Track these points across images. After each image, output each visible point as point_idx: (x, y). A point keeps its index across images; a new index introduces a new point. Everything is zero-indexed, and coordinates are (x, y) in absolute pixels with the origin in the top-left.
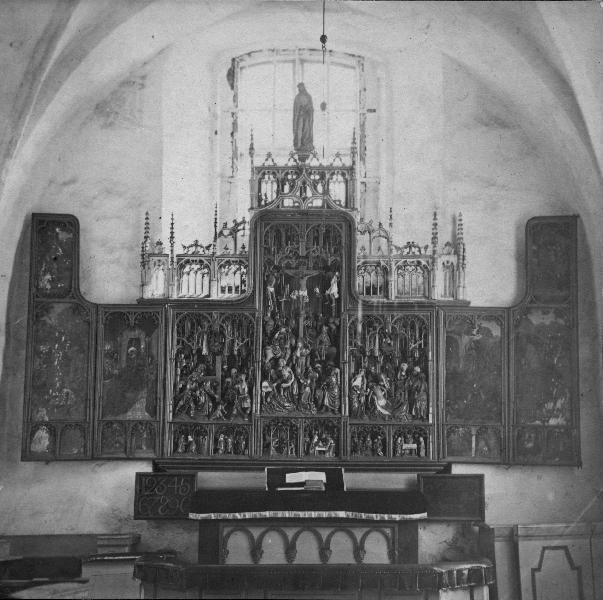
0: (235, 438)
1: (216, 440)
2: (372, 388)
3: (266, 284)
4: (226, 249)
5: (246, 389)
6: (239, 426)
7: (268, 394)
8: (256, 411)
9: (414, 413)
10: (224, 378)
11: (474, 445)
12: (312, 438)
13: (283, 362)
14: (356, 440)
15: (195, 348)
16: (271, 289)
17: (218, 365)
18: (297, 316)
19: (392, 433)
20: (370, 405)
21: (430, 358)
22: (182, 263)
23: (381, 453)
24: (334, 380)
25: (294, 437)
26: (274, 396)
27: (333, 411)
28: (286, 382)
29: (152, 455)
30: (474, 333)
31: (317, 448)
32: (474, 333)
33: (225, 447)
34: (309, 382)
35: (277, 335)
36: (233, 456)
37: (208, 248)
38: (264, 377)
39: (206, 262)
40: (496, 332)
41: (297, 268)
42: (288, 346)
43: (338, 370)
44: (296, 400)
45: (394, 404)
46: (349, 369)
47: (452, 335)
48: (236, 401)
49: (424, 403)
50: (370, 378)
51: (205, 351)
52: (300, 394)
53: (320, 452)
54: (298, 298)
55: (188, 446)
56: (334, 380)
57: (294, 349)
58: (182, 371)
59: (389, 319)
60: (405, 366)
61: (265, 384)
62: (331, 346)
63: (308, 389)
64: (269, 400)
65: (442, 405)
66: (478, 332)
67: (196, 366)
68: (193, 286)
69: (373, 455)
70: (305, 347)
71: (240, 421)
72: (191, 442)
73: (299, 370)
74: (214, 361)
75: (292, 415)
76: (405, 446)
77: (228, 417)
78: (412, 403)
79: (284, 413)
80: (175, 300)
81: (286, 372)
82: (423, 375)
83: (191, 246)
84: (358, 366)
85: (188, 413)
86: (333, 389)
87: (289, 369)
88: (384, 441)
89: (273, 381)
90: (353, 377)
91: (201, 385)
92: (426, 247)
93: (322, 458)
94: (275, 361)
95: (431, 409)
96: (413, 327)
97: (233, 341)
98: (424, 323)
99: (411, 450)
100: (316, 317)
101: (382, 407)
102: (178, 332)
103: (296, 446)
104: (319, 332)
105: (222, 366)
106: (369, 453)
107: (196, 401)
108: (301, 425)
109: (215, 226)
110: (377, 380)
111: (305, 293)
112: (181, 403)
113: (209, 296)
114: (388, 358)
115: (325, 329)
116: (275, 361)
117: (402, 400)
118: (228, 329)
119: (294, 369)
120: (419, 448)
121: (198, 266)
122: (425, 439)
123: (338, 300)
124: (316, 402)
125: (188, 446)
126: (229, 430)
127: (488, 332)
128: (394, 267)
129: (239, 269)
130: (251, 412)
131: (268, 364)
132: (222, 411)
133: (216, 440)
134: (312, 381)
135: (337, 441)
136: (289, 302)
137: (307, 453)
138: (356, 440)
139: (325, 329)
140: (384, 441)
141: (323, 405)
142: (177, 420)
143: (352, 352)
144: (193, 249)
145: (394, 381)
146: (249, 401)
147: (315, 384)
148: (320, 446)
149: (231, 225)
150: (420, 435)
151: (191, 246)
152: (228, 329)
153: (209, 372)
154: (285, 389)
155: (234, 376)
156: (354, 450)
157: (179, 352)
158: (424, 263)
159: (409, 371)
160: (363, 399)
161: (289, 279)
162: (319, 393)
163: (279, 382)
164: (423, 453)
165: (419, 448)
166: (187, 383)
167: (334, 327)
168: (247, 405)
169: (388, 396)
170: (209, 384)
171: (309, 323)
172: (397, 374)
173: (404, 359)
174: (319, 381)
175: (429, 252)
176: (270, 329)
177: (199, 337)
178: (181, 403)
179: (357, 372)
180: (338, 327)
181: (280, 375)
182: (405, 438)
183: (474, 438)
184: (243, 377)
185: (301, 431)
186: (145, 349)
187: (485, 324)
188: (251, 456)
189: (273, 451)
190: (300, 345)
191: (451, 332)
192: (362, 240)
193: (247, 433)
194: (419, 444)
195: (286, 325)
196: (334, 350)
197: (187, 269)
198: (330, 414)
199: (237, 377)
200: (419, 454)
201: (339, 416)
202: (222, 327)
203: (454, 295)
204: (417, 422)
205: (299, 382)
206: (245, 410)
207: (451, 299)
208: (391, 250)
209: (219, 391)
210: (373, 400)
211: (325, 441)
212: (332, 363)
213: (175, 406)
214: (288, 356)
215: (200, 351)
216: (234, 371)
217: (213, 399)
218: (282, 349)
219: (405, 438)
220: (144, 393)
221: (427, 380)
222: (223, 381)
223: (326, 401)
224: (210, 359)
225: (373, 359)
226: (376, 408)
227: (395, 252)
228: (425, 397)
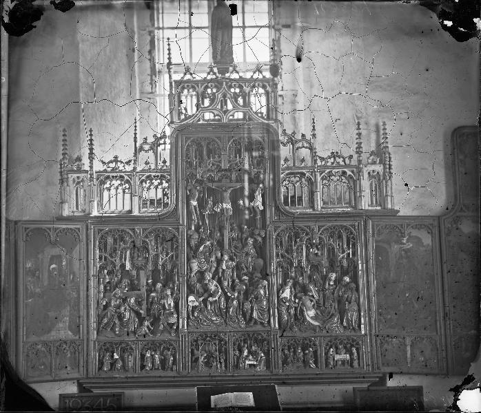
0: (162, 354)
1: (143, 356)
2: (300, 299)
3: (188, 199)
4: (147, 163)
5: (172, 304)
6: (165, 342)
7: (194, 308)
8: (183, 326)
9: (345, 324)
10: (149, 291)
11: (409, 353)
12: (241, 351)
13: (209, 276)
14: (286, 352)
15: (118, 263)
16: (194, 203)
17: (143, 281)
18: (221, 229)
19: (324, 345)
20: (299, 317)
21: (360, 268)
22: (103, 178)
23: (313, 366)
24: (262, 292)
28: (211, 295)
29: (76, 375)
30: (405, 241)
31: (247, 362)
32: (405, 241)
33: (153, 363)
34: (236, 294)
35: (201, 248)
36: (161, 373)
37: (128, 163)
38: (191, 291)
39: (126, 177)
40: (427, 240)
41: (220, 181)
42: (213, 259)
43: (266, 283)
44: (223, 313)
45: (324, 315)
46: (276, 280)
47: (380, 244)
48: (162, 317)
49: (355, 314)
50: (298, 289)
51: (128, 266)
52: (227, 308)
53: (250, 365)
54: (222, 210)
55: (113, 365)
56: (262, 292)
57: (219, 262)
58: (105, 287)
59: (316, 230)
60: (333, 276)
61: (191, 298)
62: (258, 258)
64: (196, 314)
65: (374, 315)
66: (408, 241)
67: (120, 281)
68: (115, 202)
69: (305, 367)
70: (231, 259)
71: (166, 337)
72: (117, 359)
73: (226, 284)
74: (138, 275)
76: (337, 357)
77: (152, 332)
78: (342, 313)
79: (213, 328)
80: (96, 217)
81: (212, 286)
82: (353, 285)
83: (111, 162)
84: (286, 277)
85: (113, 329)
86: (261, 301)
87: (215, 282)
88: (315, 352)
89: (198, 295)
90: (281, 288)
91: (125, 300)
92: (351, 157)
93: (252, 371)
94: (201, 274)
95: (362, 319)
96: (340, 237)
97: (157, 256)
98: (352, 233)
99: (343, 362)
100: (241, 229)
101: (312, 318)
102: (100, 249)
103: (226, 361)
104: (245, 245)
105: (147, 280)
106: (301, 364)
107: (121, 317)
108: (230, 339)
109: (135, 141)
110: (305, 290)
111: (229, 206)
112: (105, 320)
113: (130, 211)
114: (315, 267)
115: (251, 241)
116: (201, 274)
117: (333, 311)
118: (152, 244)
119: (220, 282)
120: (352, 359)
121: (119, 182)
122: (358, 350)
123: (263, 212)
124: (244, 315)
125: (113, 365)
126: (154, 346)
127: (419, 240)
128: (319, 178)
129: (161, 183)
130: (178, 327)
131: (194, 279)
132: (148, 327)
133: (143, 356)
134: (239, 293)
135: (267, 354)
136: (213, 216)
138: (286, 352)
139: (251, 241)
140: (315, 352)
142: (102, 338)
143: (279, 265)
144: (112, 165)
145: (322, 290)
146: (175, 316)
147: (242, 297)
148: (250, 360)
149: (151, 140)
150: (352, 346)
151: (111, 162)
152: (152, 244)
153: (133, 287)
154: (211, 303)
155: (159, 290)
156: (285, 362)
157: (102, 268)
158: (349, 173)
159: (338, 281)
160: (292, 311)
161: (211, 192)
163: (206, 295)
164: (356, 364)
165: (352, 359)
166: (110, 300)
167: (260, 239)
168: (173, 320)
169: (317, 306)
170: (132, 300)
171: (234, 235)
172: (324, 283)
173: (332, 268)
174: (246, 294)
175: (354, 162)
176: (193, 243)
177: (122, 252)
178: (105, 320)
179: (285, 284)
180: (264, 239)
181: (206, 289)
182: (337, 348)
183: (409, 348)
184: (169, 292)
185: (231, 344)
186: (67, 264)
187: (415, 233)
188: (179, 372)
190: (226, 257)
191: (380, 241)
192: (285, 151)
193: (174, 348)
194: (351, 354)
195: (211, 236)
196: (261, 261)
197: (107, 185)
198: (259, 327)
199: (162, 291)
200: (352, 366)
201: (268, 329)
202: (144, 242)
203: (382, 202)
204: (348, 333)
206: (171, 325)
207: (379, 208)
208: (316, 161)
209: (144, 306)
210: (302, 311)
212: (259, 275)
213: (99, 323)
214: (214, 269)
215: (123, 266)
216: (159, 285)
217: (138, 314)
218: (208, 262)
219: (337, 348)
220: (66, 311)
221: (357, 289)
222: (148, 295)
223: (255, 315)
224: (134, 273)
225: (300, 268)
226: (305, 319)
227: (319, 163)
228: (356, 308)
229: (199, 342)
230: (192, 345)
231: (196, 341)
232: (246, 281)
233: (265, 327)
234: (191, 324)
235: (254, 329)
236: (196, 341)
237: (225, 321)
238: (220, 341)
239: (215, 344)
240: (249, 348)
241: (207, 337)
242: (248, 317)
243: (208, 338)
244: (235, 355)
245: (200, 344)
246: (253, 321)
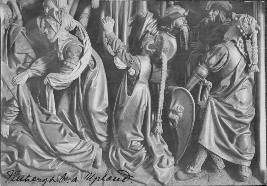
26: (21, 118)
63: (141, 90)
73: (109, 26)
86: (231, 89)
124: (170, 136)
134: (156, 62)
141: (195, 146)
162: (179, 110)
205: (109, 66)
223: (209, 138)
232: (180, 21)
246: (202, 158)
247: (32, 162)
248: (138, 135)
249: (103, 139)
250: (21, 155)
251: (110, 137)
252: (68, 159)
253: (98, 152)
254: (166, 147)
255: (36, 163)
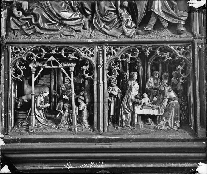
12: (124, 88)
25: (86, 87)
27: (172, 27)
31: (138, 110)
53: (145, 118)
75: (78, 38)
93: (149, 130)
103: (90, 108)
137: (115, 120)
141: (149, 13)
185: (103, 72)
189: (38, 117)
198: (166, 35)
201: (186, 37)
211: (156, 94)
229: (33, 67)
230: (17, 72)
231: (26, 64)
233: (179, 33)
234: (13, 26)
235: (153, 37)
236: (26, 64)
237: (91, 22)
238: (80, 63)
239: (67, 69)
240: (142, 81)
241: (48, 56)
242: (140, 17)
243: (52, 58)
244: (111, 95)
245: (33, 69)
246: (153, 21)
247: (44, 25)
248: (112, 7)
249: (88, 13)
250: (36, 20)
251: (93, 12)
252: (67, 23)
253: (85, 20)
254: (130, 16)
255: (46, 26)
